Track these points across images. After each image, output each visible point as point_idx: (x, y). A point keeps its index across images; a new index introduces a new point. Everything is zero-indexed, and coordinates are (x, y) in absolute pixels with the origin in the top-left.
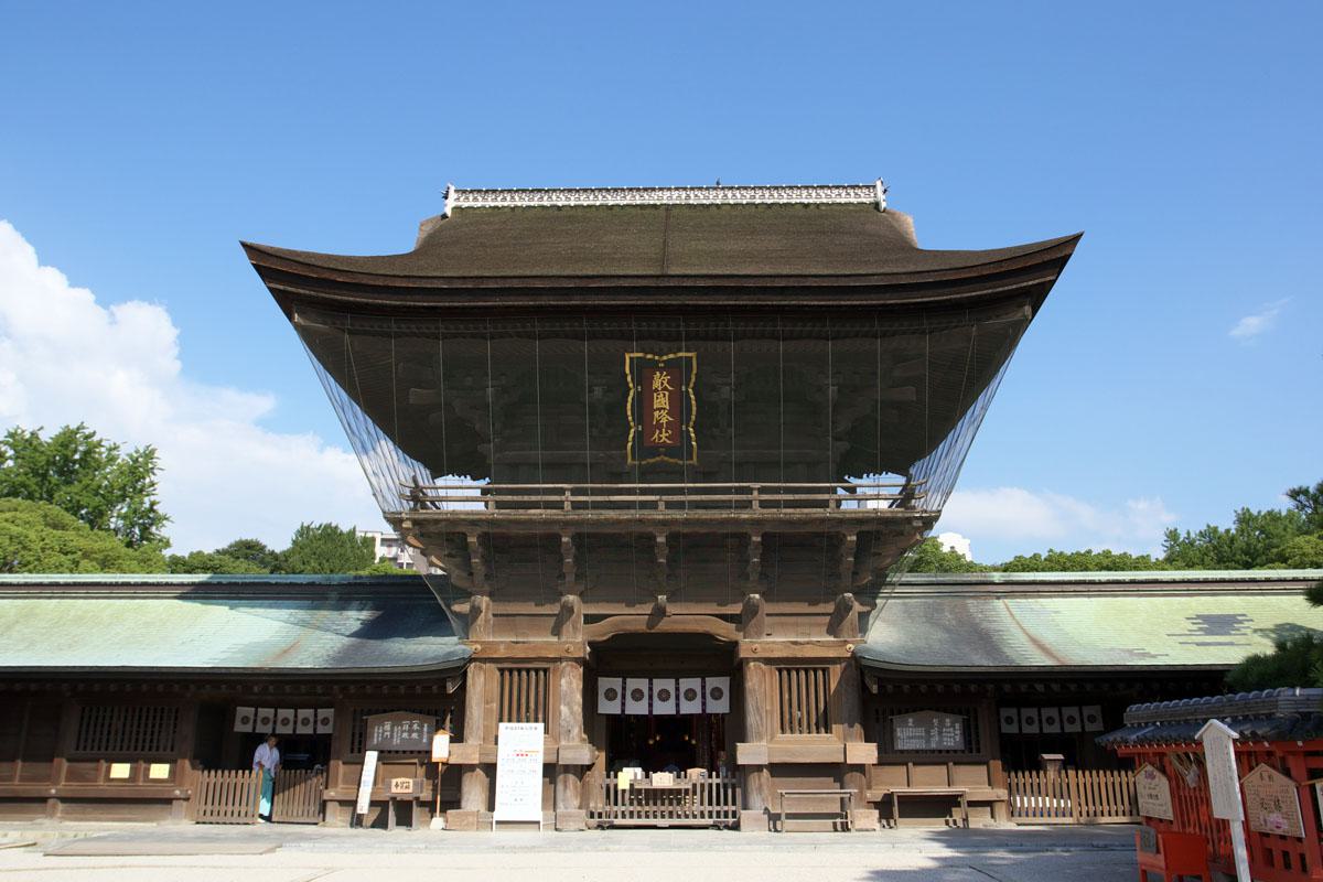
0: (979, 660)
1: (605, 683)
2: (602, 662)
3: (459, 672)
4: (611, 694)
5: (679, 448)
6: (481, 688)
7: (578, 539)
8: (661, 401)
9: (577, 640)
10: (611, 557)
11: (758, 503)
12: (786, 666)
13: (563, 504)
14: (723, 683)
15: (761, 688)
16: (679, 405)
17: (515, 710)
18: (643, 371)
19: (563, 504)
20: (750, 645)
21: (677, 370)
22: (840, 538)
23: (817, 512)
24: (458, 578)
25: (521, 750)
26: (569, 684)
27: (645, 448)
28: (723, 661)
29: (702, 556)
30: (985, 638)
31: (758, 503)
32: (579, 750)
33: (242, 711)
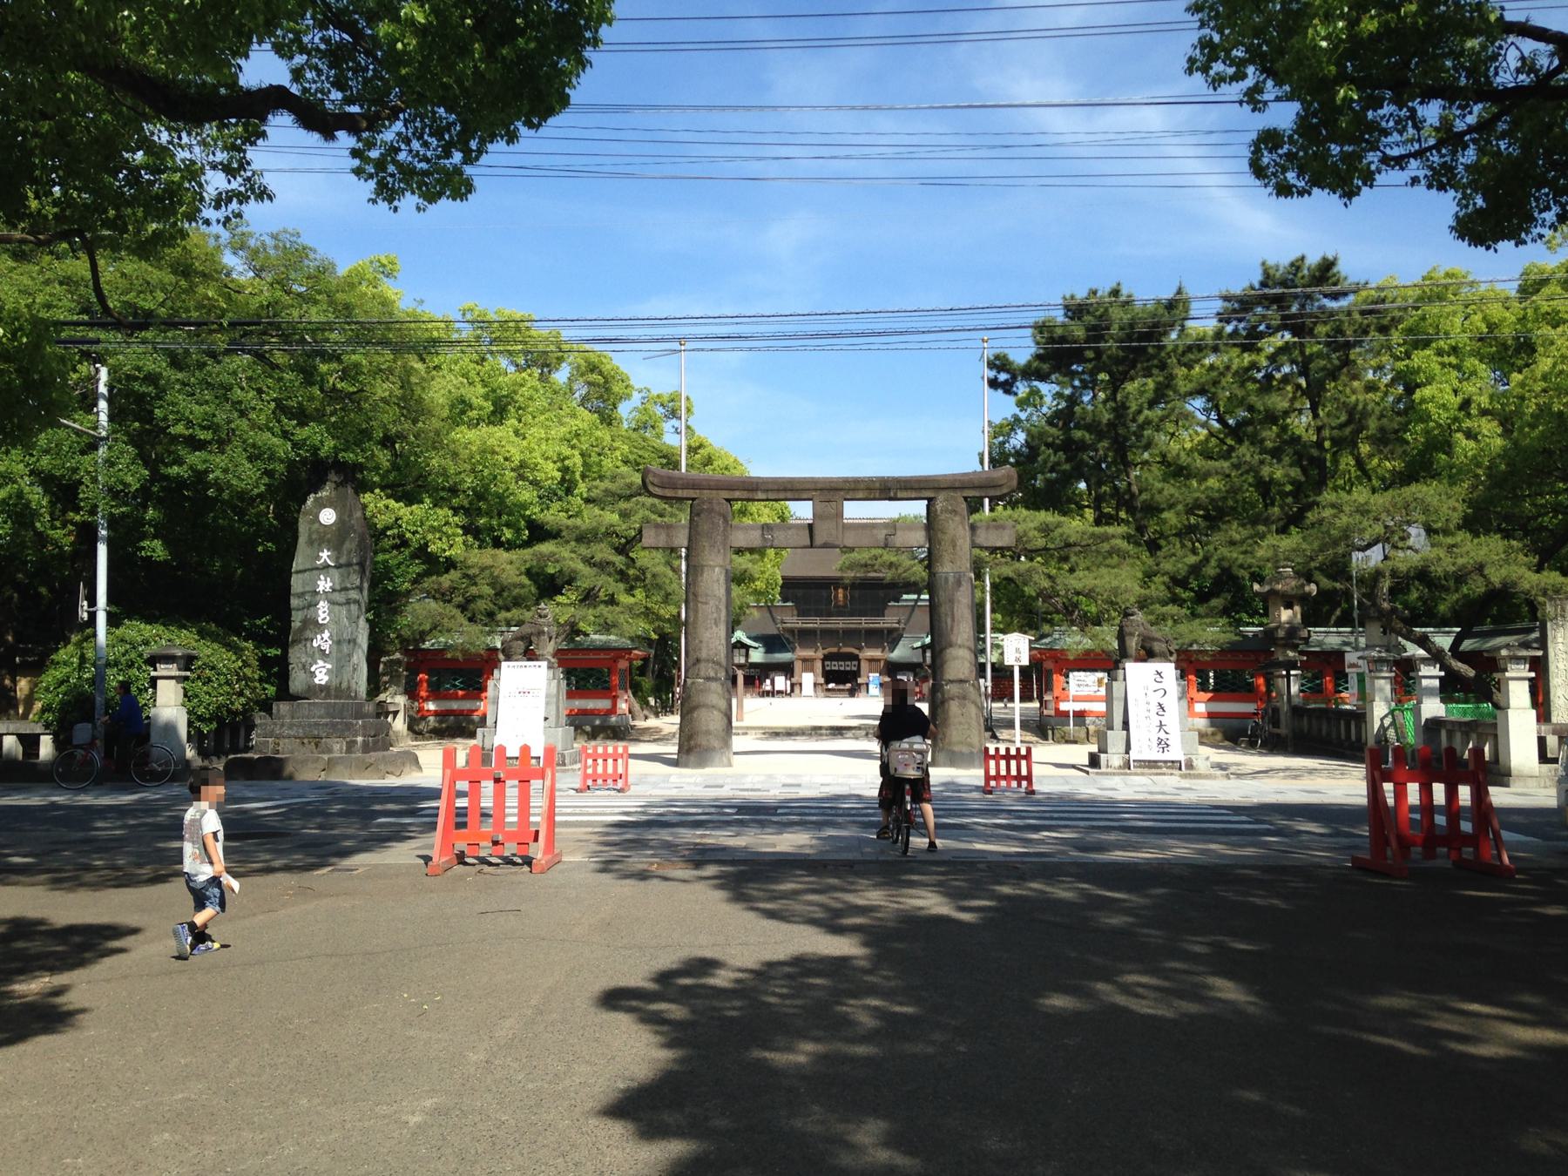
2: (826, 658)
5: (845, 606)
6: (798, 666)
9: (820, 654)
10: (828, 635)
11: (864, 623)
12: (871, 660)
13: (814, 623)
15: (864, 666)
17: (806, 670)
19: (814, 623)
20: (861, 655)
25: (808, 679)
26: (819, 665)
27: (836, 606)
28: (856, 658)
29: (850, 635)
31: (864, 623)
32: (822, 680)
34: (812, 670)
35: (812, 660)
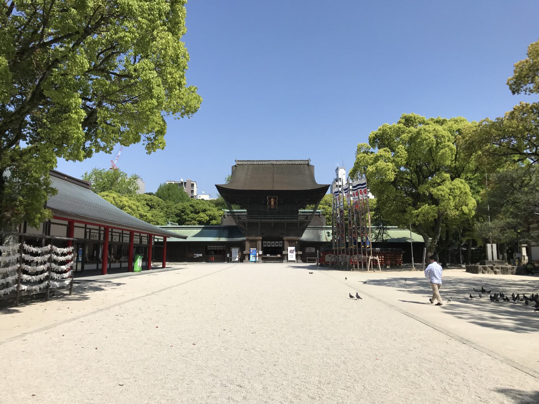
0: (316, 240)
1: (264, 242)
3: (244, 241)
4: (265, 244)
7: (261, 223)
8: (272, 202)
14: (282, 242)
15: (286, 243)
16: (275, 203)
18: (270, 199)
21: (275, 199)
22: (297, 223)
23: (294, 220)
24: (243, 228)
26: (260, 243)
30: (319, 237)
33: (209, 246)
34: (255, 247)
35: (256, 241)
